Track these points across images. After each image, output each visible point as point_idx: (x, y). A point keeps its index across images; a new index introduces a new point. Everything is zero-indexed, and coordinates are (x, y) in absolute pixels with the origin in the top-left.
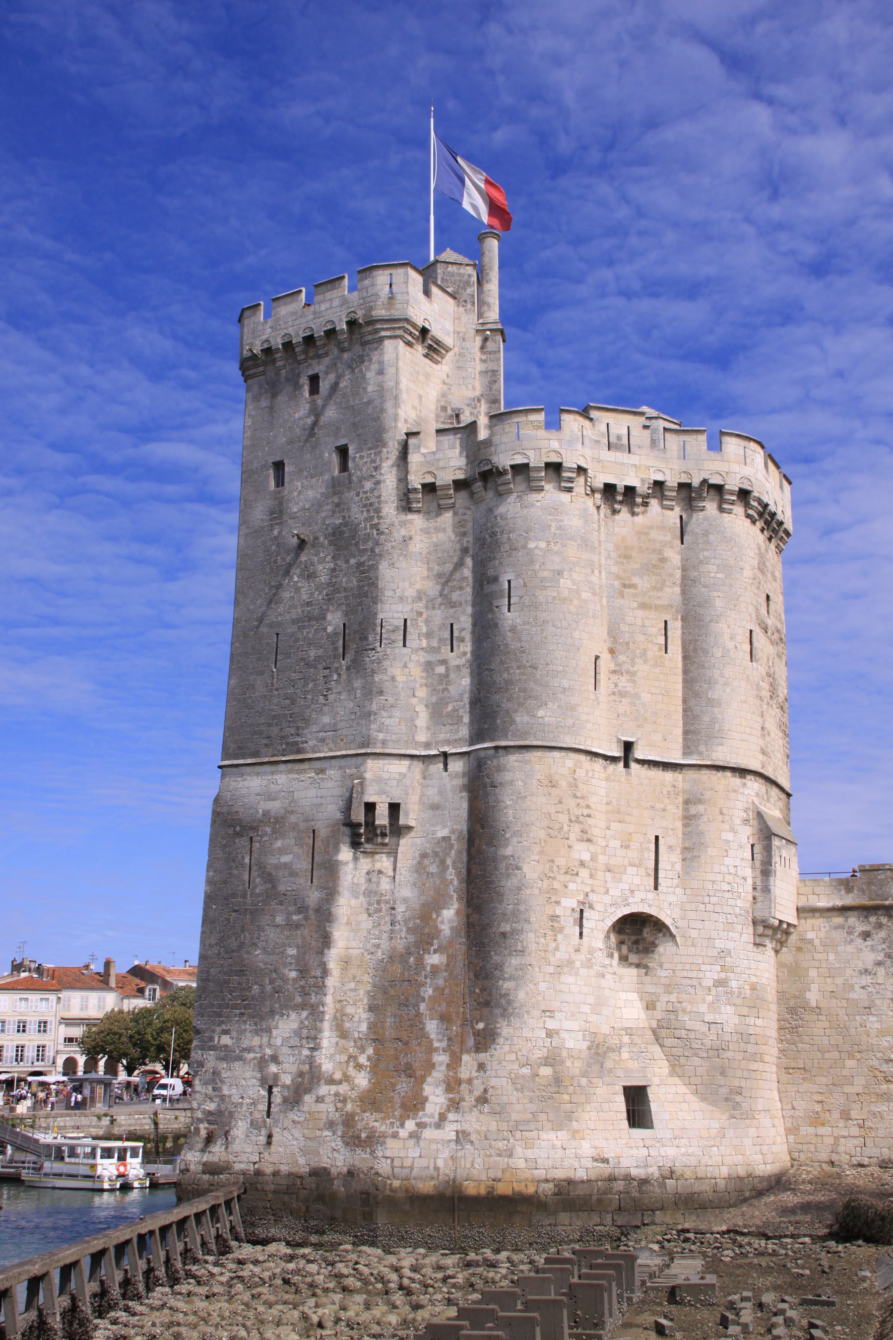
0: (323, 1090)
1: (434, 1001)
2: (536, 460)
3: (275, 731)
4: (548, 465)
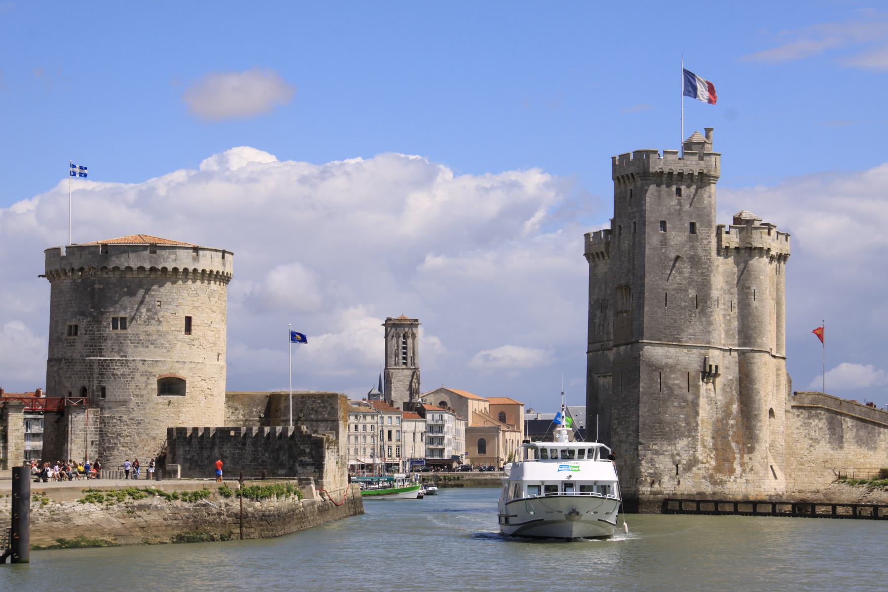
0: (700, 466)
1: (733, 436)
2: (766, 248)
3: (668, 332)
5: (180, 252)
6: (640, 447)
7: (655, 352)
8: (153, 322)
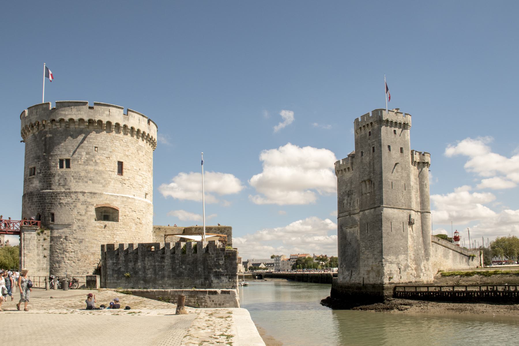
0: (410, 269)
6: (383, 260)
7: (387, 212)
8: (91, 163)
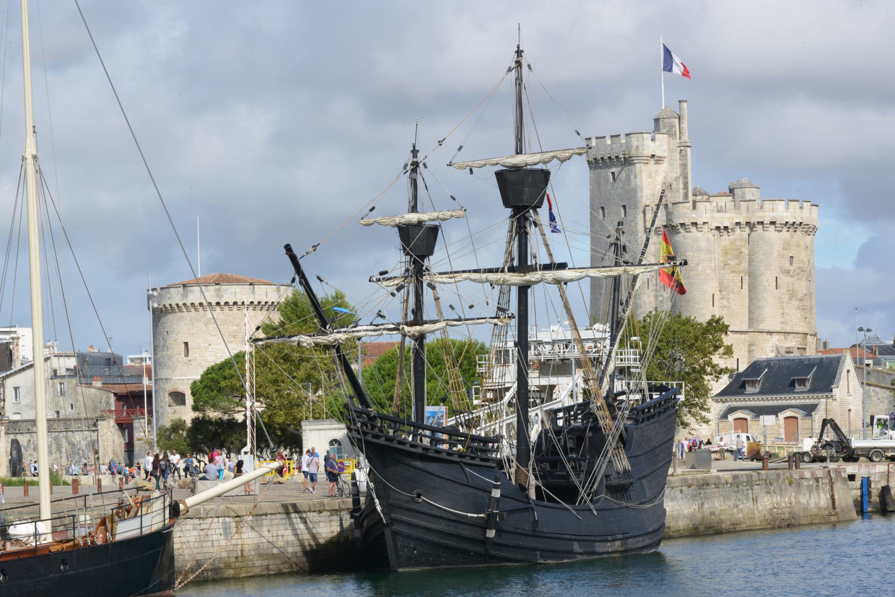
4: (692, 223)
5: (173, 290)
